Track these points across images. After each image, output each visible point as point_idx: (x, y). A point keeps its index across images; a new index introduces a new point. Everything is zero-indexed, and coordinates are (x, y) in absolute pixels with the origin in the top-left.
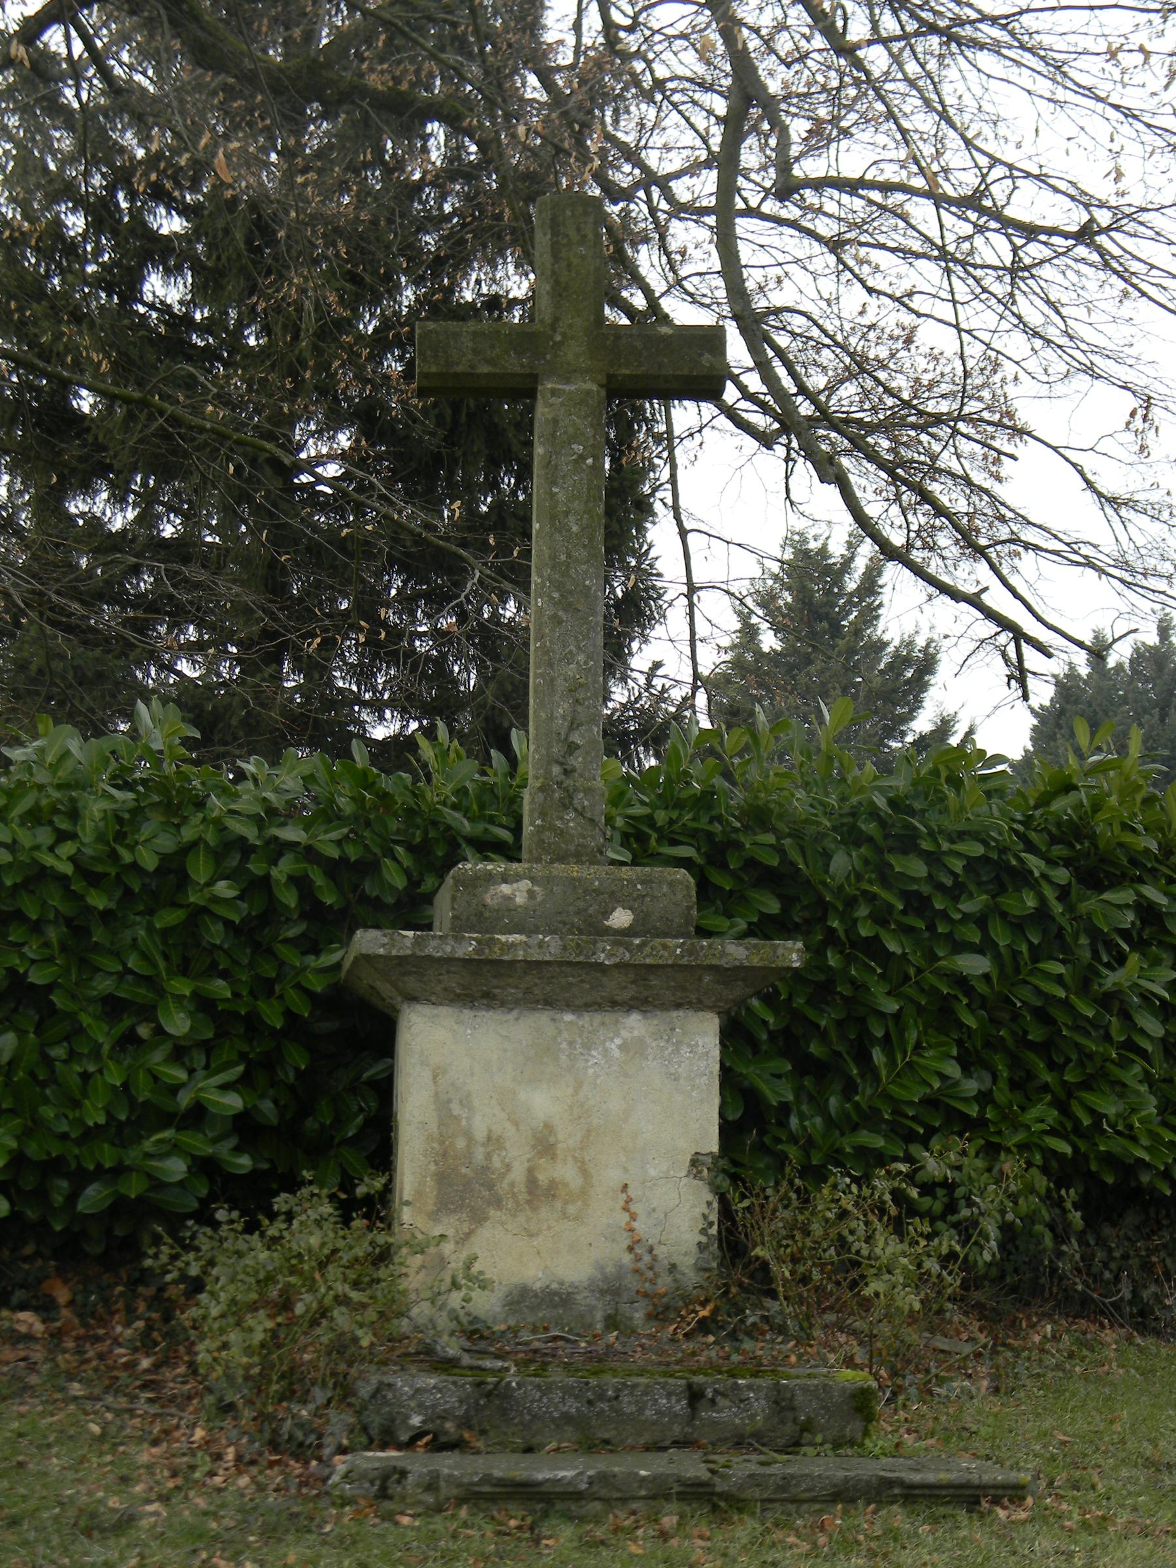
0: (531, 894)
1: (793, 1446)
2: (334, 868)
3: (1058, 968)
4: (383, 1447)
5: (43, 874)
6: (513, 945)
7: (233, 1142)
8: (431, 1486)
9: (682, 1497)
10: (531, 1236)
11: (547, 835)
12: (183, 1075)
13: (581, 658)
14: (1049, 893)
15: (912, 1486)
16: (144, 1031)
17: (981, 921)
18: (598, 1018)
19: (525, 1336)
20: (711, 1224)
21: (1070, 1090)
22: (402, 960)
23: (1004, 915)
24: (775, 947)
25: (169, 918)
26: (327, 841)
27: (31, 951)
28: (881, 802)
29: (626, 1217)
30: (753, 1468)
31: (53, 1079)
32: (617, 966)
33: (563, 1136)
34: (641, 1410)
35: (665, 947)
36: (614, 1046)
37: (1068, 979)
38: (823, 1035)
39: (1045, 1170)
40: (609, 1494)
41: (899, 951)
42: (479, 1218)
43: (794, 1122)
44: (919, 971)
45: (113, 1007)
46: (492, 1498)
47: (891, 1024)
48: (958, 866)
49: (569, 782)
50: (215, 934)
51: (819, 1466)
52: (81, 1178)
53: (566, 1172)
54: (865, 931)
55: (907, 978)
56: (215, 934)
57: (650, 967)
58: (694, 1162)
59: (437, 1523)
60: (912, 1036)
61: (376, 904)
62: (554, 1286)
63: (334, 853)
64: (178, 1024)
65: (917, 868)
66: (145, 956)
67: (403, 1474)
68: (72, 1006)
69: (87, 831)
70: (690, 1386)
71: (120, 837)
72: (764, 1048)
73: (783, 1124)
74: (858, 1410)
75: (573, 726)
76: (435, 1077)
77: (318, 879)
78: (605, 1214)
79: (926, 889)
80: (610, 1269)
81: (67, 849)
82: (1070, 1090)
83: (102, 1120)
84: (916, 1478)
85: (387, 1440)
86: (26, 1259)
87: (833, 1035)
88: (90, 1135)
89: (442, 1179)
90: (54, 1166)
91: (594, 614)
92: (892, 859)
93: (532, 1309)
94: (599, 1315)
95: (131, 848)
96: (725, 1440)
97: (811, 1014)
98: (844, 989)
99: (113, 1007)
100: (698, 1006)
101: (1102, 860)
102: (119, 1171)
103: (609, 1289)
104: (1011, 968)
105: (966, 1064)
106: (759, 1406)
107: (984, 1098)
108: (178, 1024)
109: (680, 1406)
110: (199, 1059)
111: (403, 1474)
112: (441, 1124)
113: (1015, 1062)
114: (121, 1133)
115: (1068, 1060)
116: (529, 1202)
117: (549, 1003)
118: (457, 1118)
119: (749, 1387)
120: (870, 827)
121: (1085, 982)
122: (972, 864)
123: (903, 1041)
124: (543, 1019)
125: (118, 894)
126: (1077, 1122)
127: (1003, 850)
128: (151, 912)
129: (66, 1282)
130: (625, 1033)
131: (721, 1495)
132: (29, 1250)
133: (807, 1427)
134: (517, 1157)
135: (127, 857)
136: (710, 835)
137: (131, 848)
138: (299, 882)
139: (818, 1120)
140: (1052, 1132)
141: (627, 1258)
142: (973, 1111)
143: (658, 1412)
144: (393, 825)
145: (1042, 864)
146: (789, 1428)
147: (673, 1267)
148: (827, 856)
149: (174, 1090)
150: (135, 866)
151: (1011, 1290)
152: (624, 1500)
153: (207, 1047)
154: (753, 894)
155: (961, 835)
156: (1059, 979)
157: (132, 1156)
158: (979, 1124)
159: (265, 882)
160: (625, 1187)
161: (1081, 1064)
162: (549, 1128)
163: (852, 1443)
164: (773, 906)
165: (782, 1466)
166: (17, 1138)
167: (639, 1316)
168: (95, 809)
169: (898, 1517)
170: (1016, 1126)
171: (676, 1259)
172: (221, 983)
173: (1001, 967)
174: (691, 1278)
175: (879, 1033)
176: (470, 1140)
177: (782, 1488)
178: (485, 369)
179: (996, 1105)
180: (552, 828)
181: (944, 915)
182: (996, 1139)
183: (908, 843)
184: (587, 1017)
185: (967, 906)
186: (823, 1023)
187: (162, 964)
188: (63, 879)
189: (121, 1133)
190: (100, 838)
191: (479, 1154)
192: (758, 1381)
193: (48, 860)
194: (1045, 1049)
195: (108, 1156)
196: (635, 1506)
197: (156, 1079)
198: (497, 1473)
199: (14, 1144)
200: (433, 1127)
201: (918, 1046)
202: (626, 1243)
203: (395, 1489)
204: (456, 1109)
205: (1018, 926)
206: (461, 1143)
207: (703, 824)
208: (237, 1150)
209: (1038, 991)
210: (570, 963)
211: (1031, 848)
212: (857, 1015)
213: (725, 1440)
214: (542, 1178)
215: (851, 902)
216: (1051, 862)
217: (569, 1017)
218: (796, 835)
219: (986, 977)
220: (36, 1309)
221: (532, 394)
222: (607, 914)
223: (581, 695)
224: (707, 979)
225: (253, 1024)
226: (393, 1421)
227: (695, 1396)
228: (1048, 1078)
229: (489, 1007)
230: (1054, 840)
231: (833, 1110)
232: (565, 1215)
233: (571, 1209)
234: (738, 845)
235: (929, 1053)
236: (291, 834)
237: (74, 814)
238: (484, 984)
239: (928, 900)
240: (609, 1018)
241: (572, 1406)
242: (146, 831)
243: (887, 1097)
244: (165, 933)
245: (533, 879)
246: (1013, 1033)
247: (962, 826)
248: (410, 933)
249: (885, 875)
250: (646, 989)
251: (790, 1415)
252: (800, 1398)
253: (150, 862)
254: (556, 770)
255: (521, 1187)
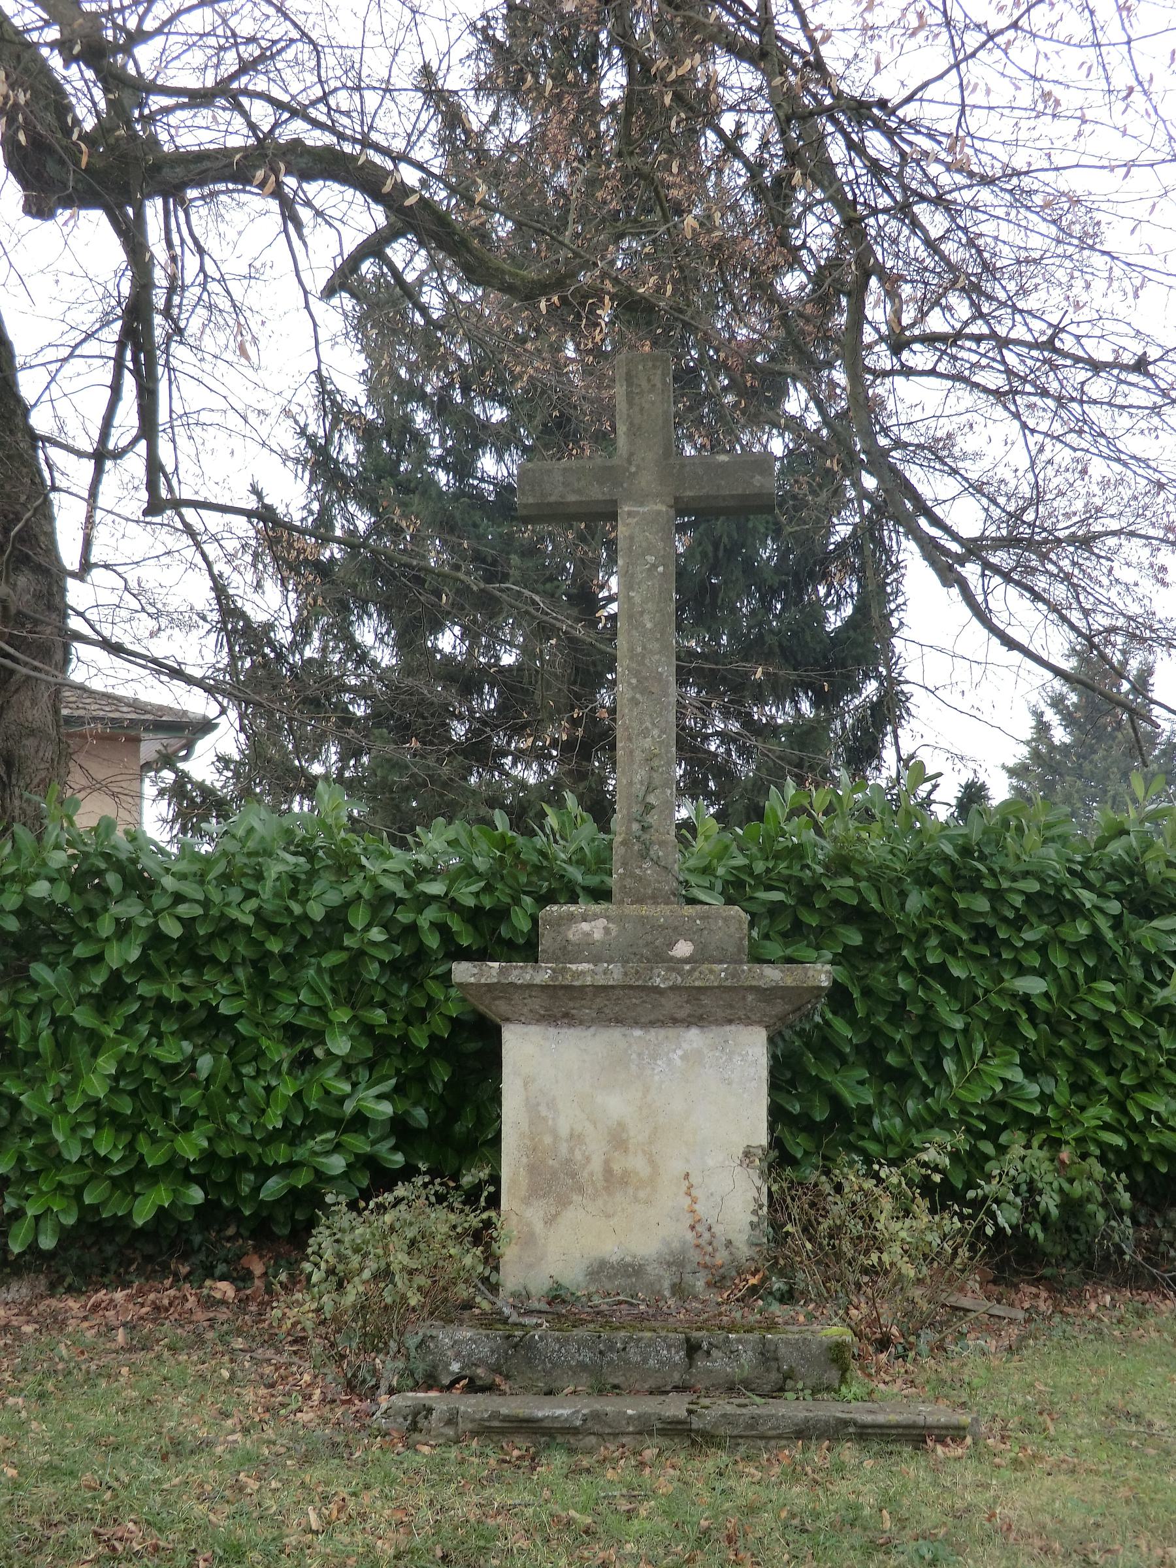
0: (607, 930)
1: (779, 1391)
2: (473, 916)
3: (1110, 987)
4: (429, 1388)
5: (234, 926)
6: (582, 973)
7: (392, 1142)
8: (451, 1421)
9: (663, 1432)
10: (608, 1216)
11: (628, 882)
12: (347, 1088)
13: (656, 732)
14: (1103, 924)
15: (865, 1426)
16: (319, 1052)
17: (1042, 948)
18: (662, 1033)
19: (596, 1300)
20: (761, 1207)
21: (1127, 1092)
22: (490, 987)
23: (1063, 942)
24: (806, 970)
25: (333, 959)
26: (467, 895)
27: (223, 988)
28: (948, 849)
29: (688, 1200)
30: (729, 1409)
31: (242, 1093)
32: (671, 988)
33: (639, 1133)
34: (645, 1361)
35: (711, 971)
36: (676, 1057)
37: (1120, 996)
38: (901, 1049)
39: (1103, 1160)
40: (598, 1428)
41: (963, 976)
42: (563, 1202)
43: (876, 1122)
44: (986, 991)
45: (292, 1033)
46: (502, 1432)
47: (960, 1038)
48: (1018, 901)
49: (646, 836)
50: (372, 971)
51: (792, 1409)
52: (265, 1172)
53: (637, 1163)
54: (932, 959)
55: (976, 998)
56: (372, 971)
57: (699, 988)
58: (747, 1154)
59: (453, 1453)
60: (979, 1048)
61: (510, 944)
62: (628, 1259)
63: (470, 902)
64: (341, 1045)
65: (982, 904)
66: (314, 991)
67: (430, 1410)
68: (256, 1033)
69: (266, 890)
70: (688, 1340)
71: (293, 894)
72: (851, 1059)
73: (868, 1124)
74: (834, 1361)
75: (650, 789)
76: (526, 1084)
77: (455, 924)
78: (670, 1198)
79: (991, 922)
80: (676, 1245)
81: (253, 904)
82: (1127, 1092)
83: (279, 1125)
84: (869, 1419)
85: (430, 1382)
86: (229, 1239)
87: (909, 1047)
88: (273, 1137)
89: (532, 1169)
90: (240, 1163)
91: (666, 695)
92: (957, 897)
93: (609, 1278)
94: (666, 1284)
95: (303, 903)
96: (716, 1387)
97: (888, 1029)
98: (915, 1009)
99: (292, 1033)
100: (748, 1021)
101: (1154, 894)
102: (292, 1166)
103: (676, 1262)
104: (1069, 991)
105: (1030, 1072)
106: (747, 1357)
107: (1045, 1099)
108: (341, 1045)
109: (679, 1356)
110: (363, 1075)
111: (430, 1410)
112: (531, 1123)
113: (1077, 1068)
114: (291, 1134)
115: (1125, 1066)
116: (606, 1188)
117: (619, 1021)
118: (545, 1119)
119: (739, 1341)
120: (939, 870)
121: (1138, 999)
122: (1029, 898)
123: (971, 1053)
124: (615, 1035)
125: (295, 940)
126: (1132, 1119)
127: (1059, 887)
128: (321, 954)
129: (261, 1257)
130: (685, 1046)
131: (697, 1431)
132: (231, 1231)
133: (789, 1376)
134: (596, 1150)
135: (297, 909)
136: (800, 881)
137: (303, 903)
138: (442, 928)
139: (898, 1121)
140: (1106, 1127)
141: (690, 1236)
142: (1036, 1111)
143: (660, 1362)
144: (523, 879)
145: (1094, 897)
146: (774, 1376)
147: (729, 1243)
148: (903, 895)
149: (341, 1100)
150: (305, 917)
151: (1028, 1259)
152: (616, 1435)
153: (371, 1065)
154: (841, 930)
155: (1026, 874)
156: (1113, 998)
157: (301, 1153)
158: (1043, 1121)
159: (413, 928)
160: (687, 1175)
161: (1136, 1069)
162: (622, 1126)
163: (829, 1389)
164: (856, 939)
165: (759, 1407)
166: (210, 1140)
167: (700, 1284)
168: (273, 870)
169: (848, 1452)
170: (1075, 1123)
171: (731, 1236)
172: (380, 1012)
173: (1061, 988)
174: (744, 1252)
175: (949, 1045)
176: (556, 1137)
177: (752, 1427)
178: (572, 498)
179: (1057, 1106)
180: (632, 875)
181: (1007, 943)
182: (1057, 1135)
183: (974, 885)
184: (653, 1032)
185: (1029, 935)
186: (898, 1037)
187: (329, 998)
188: (247, 929)
189: (291, 1134)
190: (277, 895)
191: (564, 1149)
192: (749, 1336)
193: (234, 913)
194: (1105, 1055)
195: (280, 1154)
196: (624, 1440)
197: (327, 1092)
198: (504, 1411)
199: (205, 1144)
200: (525, 1126)
201: (984, 1055)
202: (690, 1222)
203: (423, 1423)
204: (544, 1112)
205: (1075, 952)
206: (548, 1140)
207: (796, 871)
208: (395, 1149)
209: (1096, 1009)
210: (631, 987)
211: (1088, 885)
212: (929, 1030)
213: (716, 1387)
214: (616, 1167)
215: (924, 935)
216: (1101, 895)
217: (638, 1033)
218: (874, 880)
219: (1046, 995)
220: (233, 1281)
221: (613, 517)
222: (671, 945)
223: (656, 763)
224: (750, 998)
225: (407, 1049)
226: (435, 1367)
227: (692, 1349)
228: (1105, 1082)
229: (570, 1025)
230: (1109, 877)
231: (910, 1113)
232: (636, 1200)
233: (642, 1194)
234: (822, 887)
235: (996, 1061)
236: (436, 888)
237: (259, 877)
238: (563, 1006)
239: (993, 932)
240: (671, 1032)
241: (586, 1356)
242: (316, 890)
243: (955, 1099)
244: (333, 971)
245: (607, 918)
246: (1074, 1044)
247: (1023, 867)
248: (496, 965)
249: (955, 914)
250: (699, 1006)
251: (774, 1365)
252: (783, 1350)
253: (317, 912)
254: (635, 826)
255: (599, 1176)
